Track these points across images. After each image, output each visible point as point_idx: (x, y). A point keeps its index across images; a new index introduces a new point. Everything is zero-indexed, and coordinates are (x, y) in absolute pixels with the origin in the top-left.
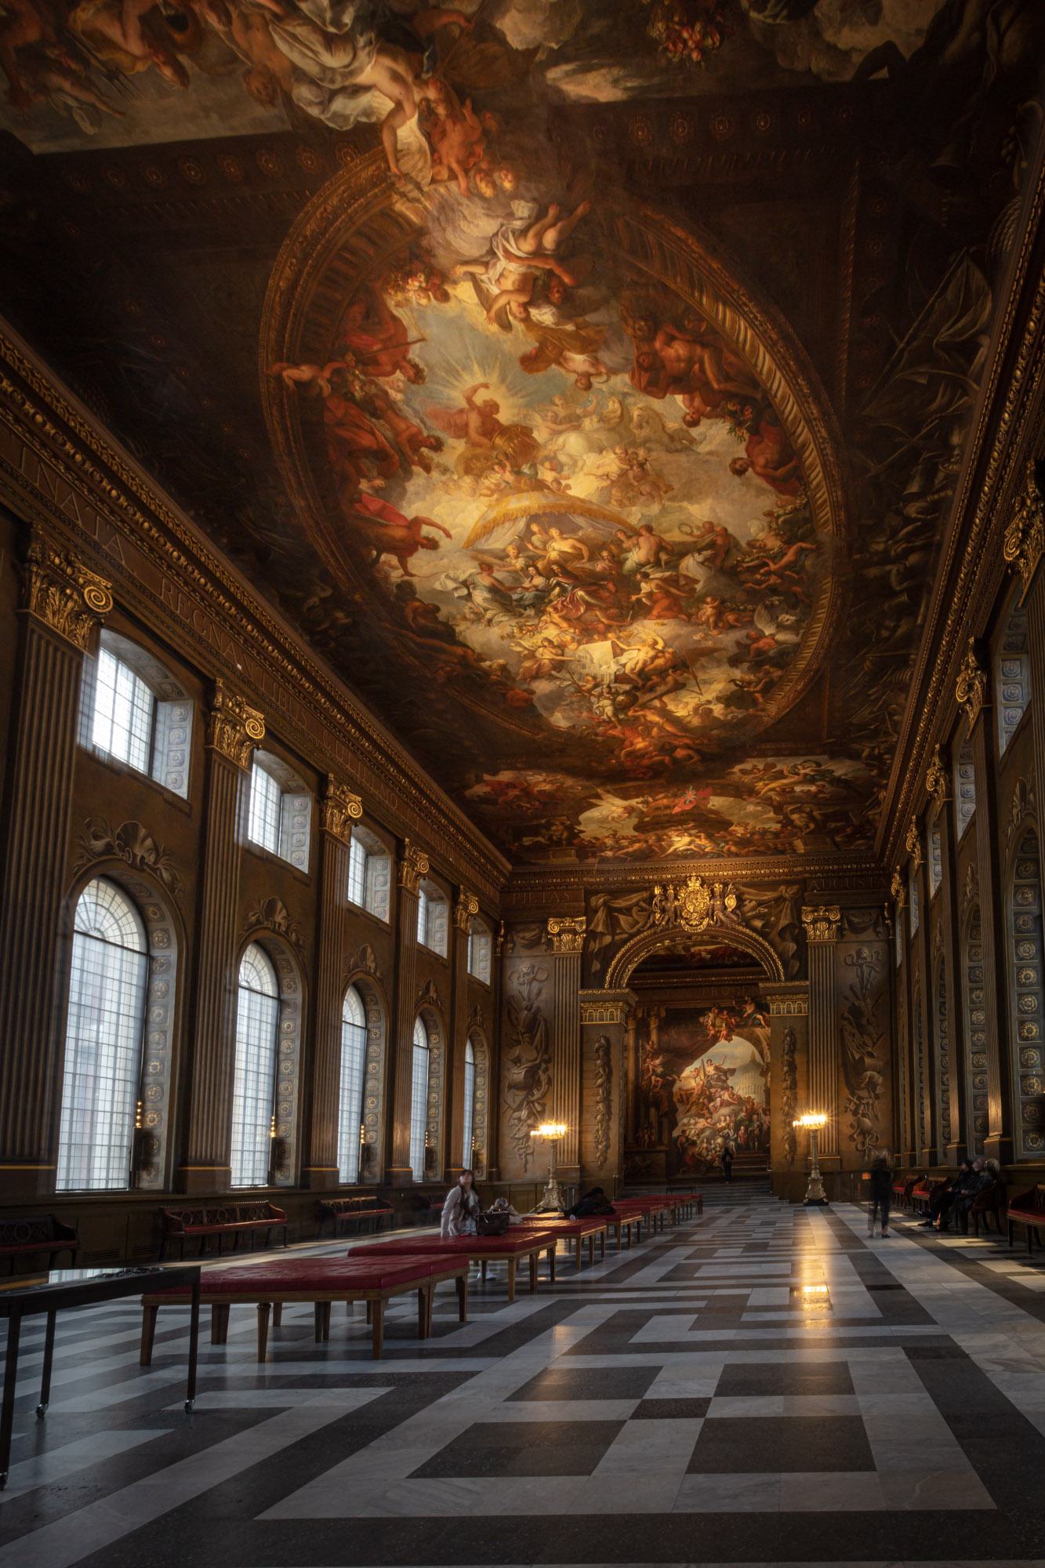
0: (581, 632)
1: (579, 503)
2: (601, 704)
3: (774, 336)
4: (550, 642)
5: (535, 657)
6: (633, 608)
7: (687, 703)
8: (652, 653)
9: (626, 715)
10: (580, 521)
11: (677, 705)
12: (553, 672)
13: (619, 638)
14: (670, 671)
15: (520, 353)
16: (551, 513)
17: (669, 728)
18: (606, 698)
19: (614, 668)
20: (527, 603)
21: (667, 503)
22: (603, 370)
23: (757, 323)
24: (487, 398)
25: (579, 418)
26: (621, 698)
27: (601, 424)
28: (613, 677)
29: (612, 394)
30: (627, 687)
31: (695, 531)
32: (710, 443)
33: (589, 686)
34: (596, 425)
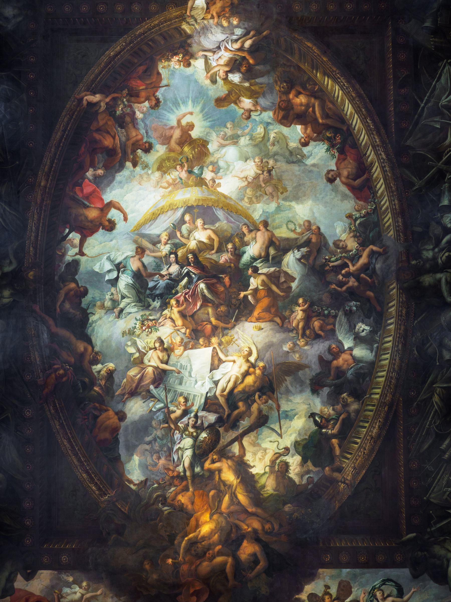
0: (190, 334)
1: (223, 199)
2: (181, 446)
3: (354, 95)
4: (162, 342)
5: (142, 362)
6: (239, 308)
7: (265, 450)
8: (245, 367)
9: (202, 467)
10: (220, 214)
11: (255, 454)
12: (152, 387)
13: (220, 344)
14: (257, 396)
15: (216, 96)
16: (202, 205)
17: (242, 498)
18: (191, 435)
19: (208, 385)
20: (158, 292)
21: (282, 202)
22: (259, 108)
23: (345, 87)
24: (189, 121)
25: (238, 137)
26: (204, 435)
27: (250, 142)
28: (203, 401)
29: (261, 123)
30: (212, 418)
31: (297, 228)
32: (314, 158)
33: (179, 412)
34: (247, 142)
